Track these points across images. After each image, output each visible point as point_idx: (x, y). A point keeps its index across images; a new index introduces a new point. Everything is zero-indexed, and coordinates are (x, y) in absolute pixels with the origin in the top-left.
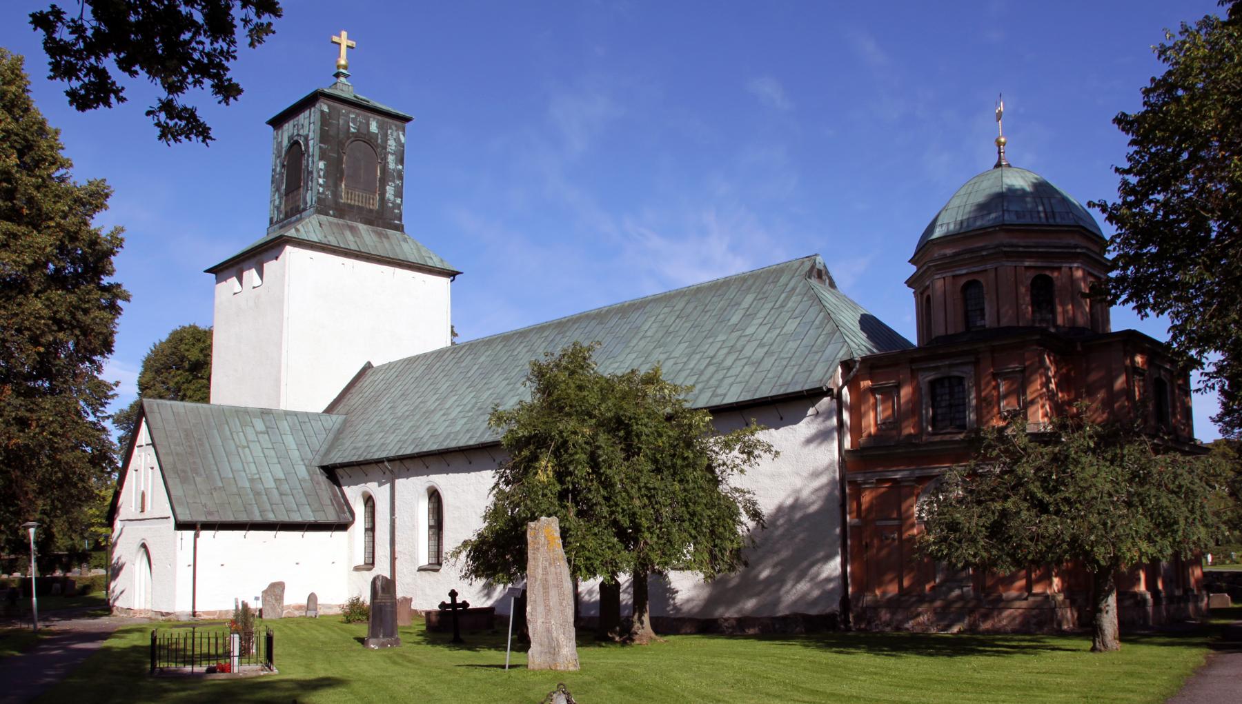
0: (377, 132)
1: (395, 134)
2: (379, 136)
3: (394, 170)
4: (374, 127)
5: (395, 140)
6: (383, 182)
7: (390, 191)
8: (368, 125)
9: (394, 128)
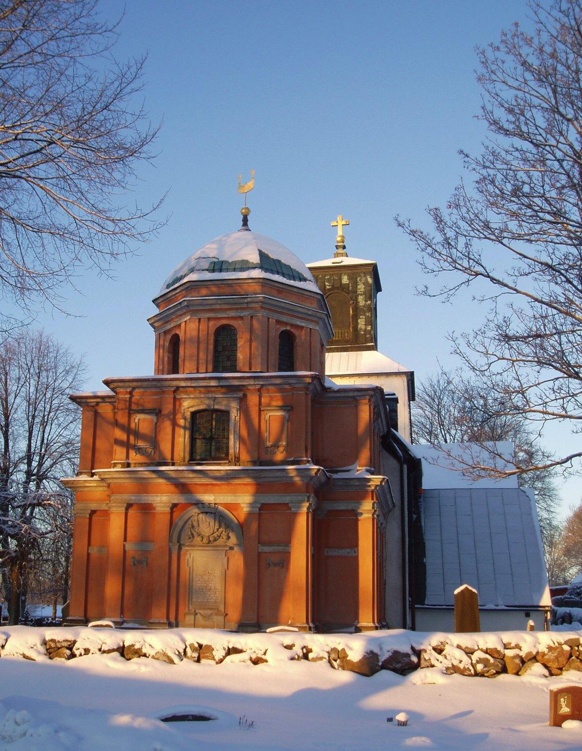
0: (348, 282)
1: (364, 279)
2: (350, 285)
3: (364, 306)
4: (345, 280)
5: (364, 283)
6: (356, 317)
7: (361, 323)
8: (340, 279)
9: (362, 275)
